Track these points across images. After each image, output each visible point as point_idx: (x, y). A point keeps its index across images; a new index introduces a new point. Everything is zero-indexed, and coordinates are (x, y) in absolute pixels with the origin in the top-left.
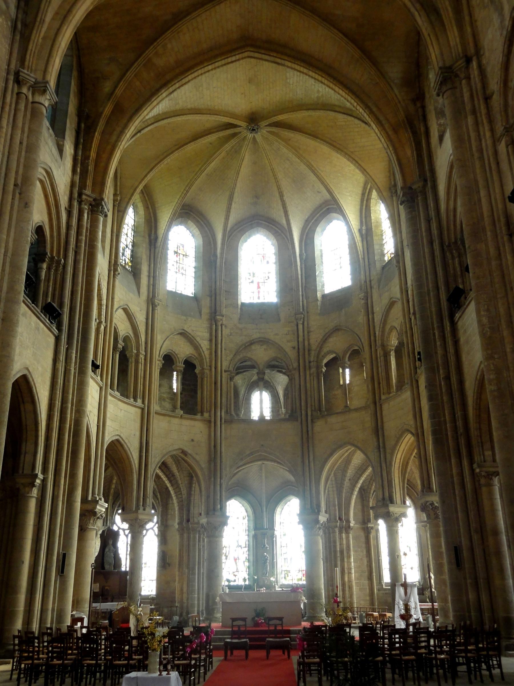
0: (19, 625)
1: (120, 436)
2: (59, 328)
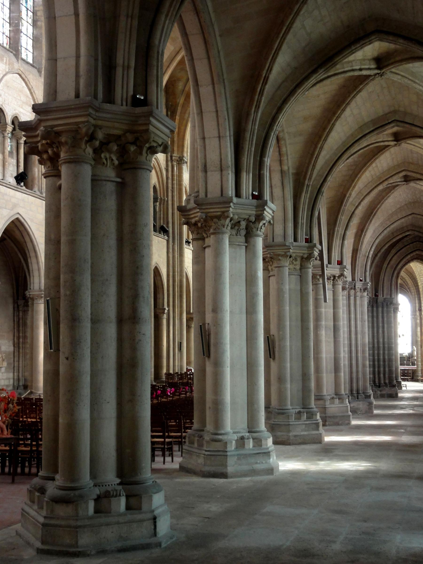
0: (165, 371)
2: (168, 236)
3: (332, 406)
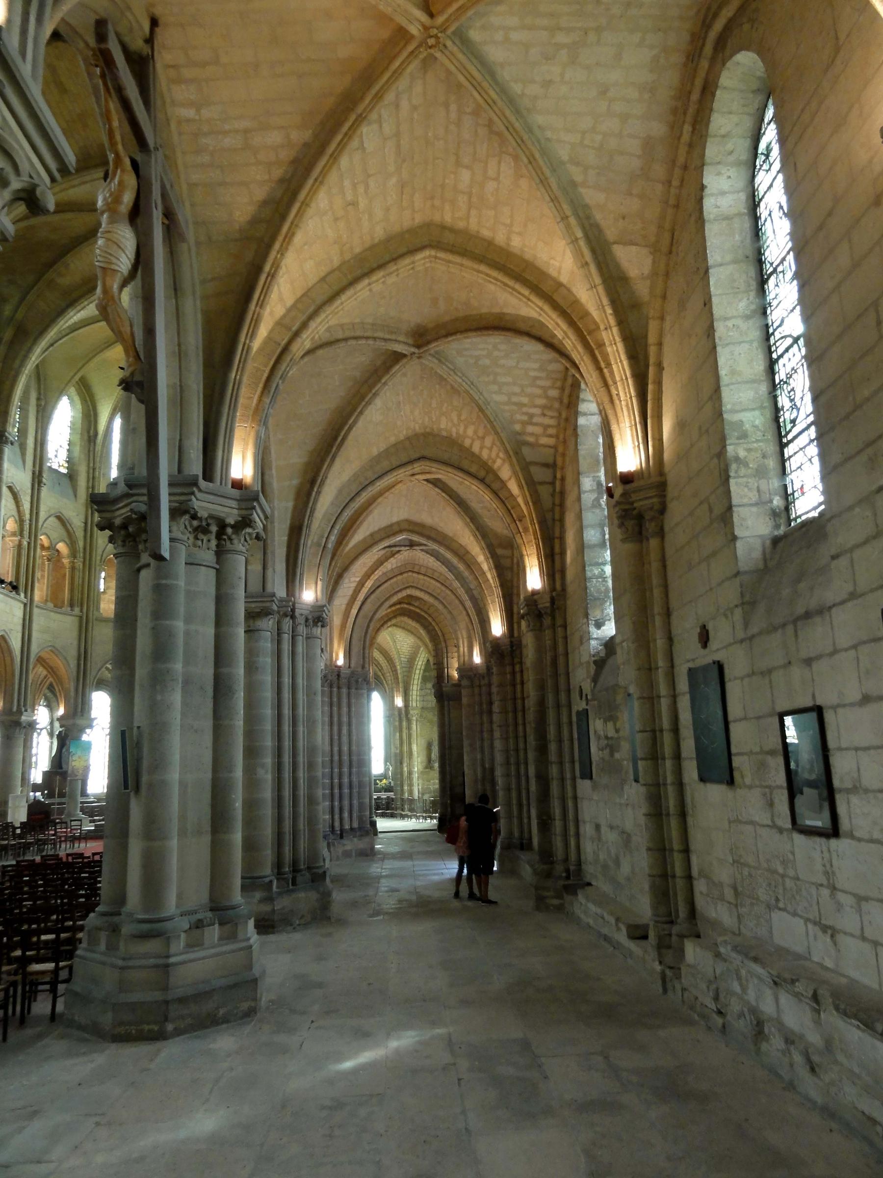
1: (54, 647)
3: (191, 956)
